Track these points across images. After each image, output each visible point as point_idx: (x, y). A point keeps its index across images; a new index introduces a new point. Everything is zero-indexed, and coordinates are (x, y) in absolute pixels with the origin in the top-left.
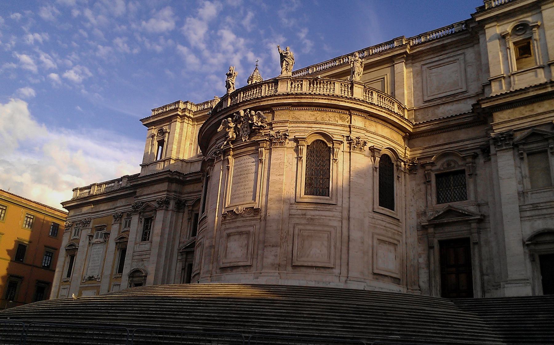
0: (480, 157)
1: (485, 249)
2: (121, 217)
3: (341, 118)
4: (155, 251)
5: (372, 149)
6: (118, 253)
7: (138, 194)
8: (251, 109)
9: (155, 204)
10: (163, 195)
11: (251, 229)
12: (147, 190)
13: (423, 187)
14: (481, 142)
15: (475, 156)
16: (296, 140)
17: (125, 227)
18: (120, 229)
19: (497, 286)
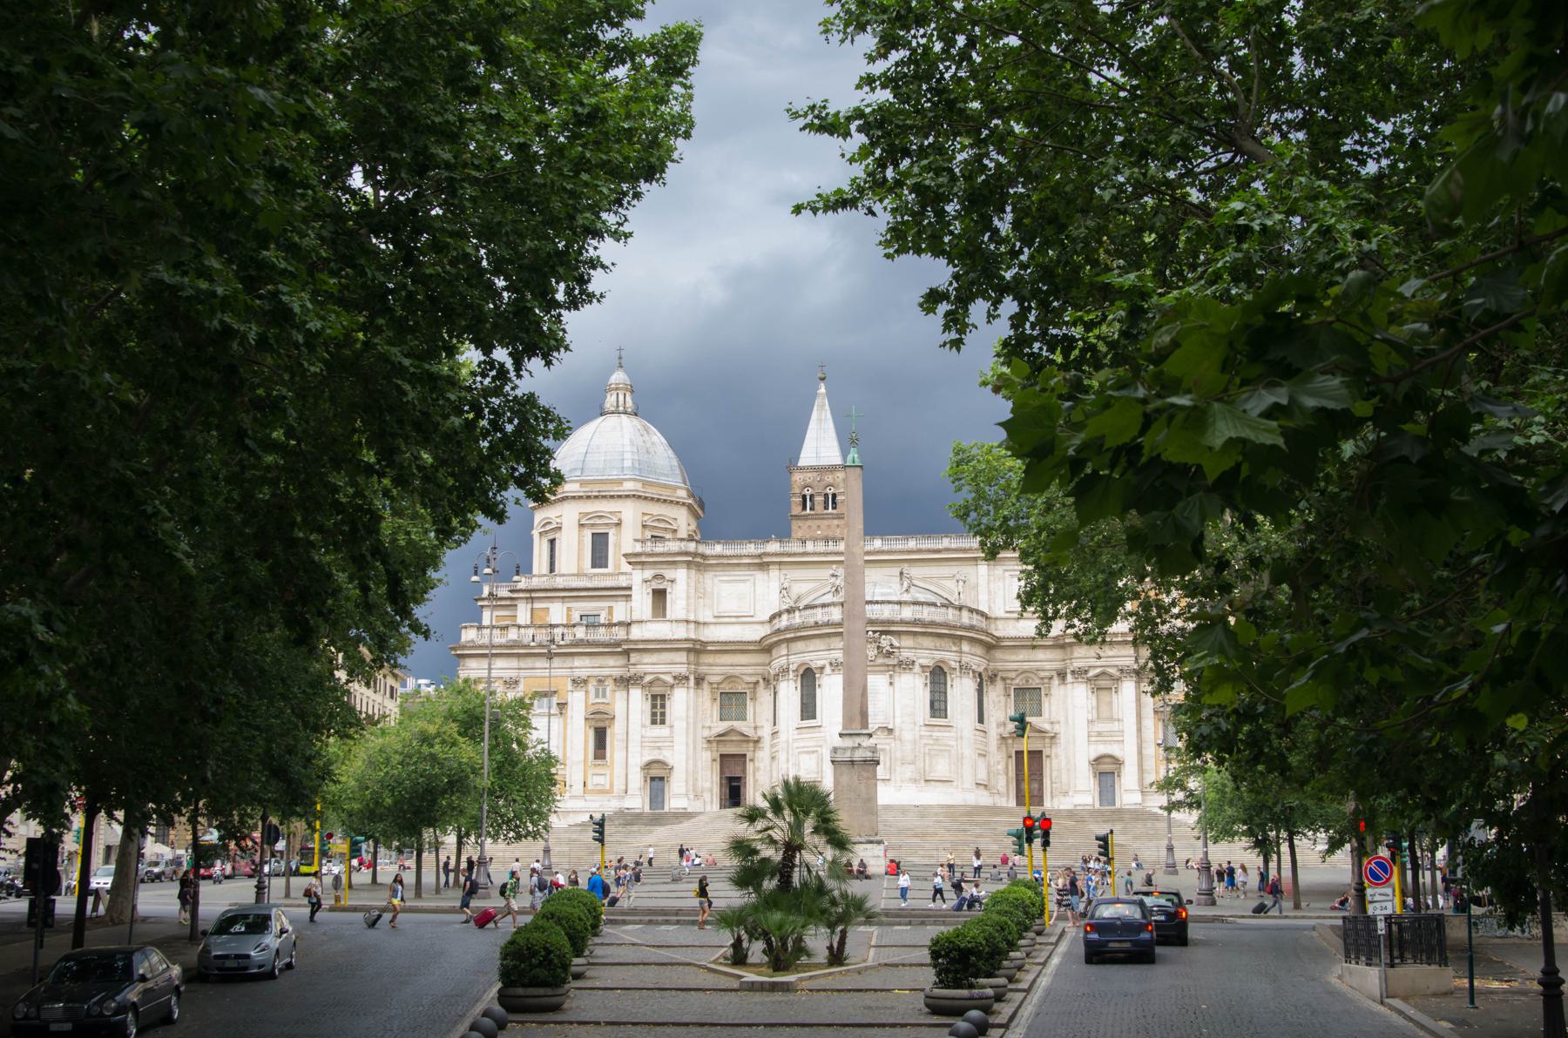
0: (1056, 678)
1: (1054, 761)
2: (585, 682)
3: (955, 644)
4: (680, 739)
5: (974, 672)
6: (591, 734)
7: (633, 660)
8: (882, 633)
9: (669, 679)
10: (682, 670)
11: (887, 747)
12: (647, 658)
13: (1003, 699)
14: (1058, 665)
15: (1051, 678)
16: (922, 666)
17: (597, 696)
19: (1066, 793)
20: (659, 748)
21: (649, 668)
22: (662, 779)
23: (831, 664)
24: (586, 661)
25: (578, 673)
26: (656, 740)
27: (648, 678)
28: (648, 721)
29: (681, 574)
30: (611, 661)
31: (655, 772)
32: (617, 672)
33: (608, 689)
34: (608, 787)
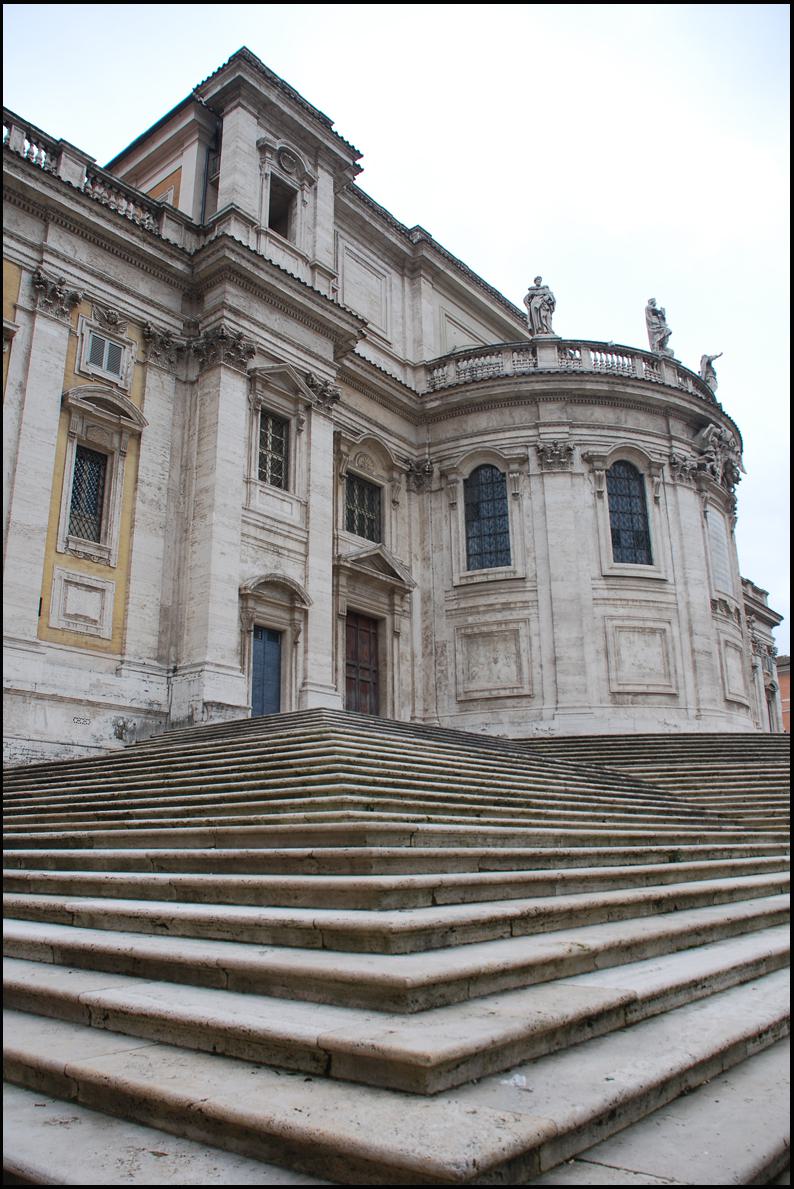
17: (96, 358)
18: (71, 353)
20: (277, 550)
21: (262, 339)
22: (275, 635)
23: (673, 464)
24: (82, 252)
25: (53, 268)
26: (271, 525)
27: (256, 363)
28: (255, 475)
29: (325, 181)
30: (144, 286)
31: (272, 615)
32: (159, 321)
33: (130, 356)
34: (106, 633)
